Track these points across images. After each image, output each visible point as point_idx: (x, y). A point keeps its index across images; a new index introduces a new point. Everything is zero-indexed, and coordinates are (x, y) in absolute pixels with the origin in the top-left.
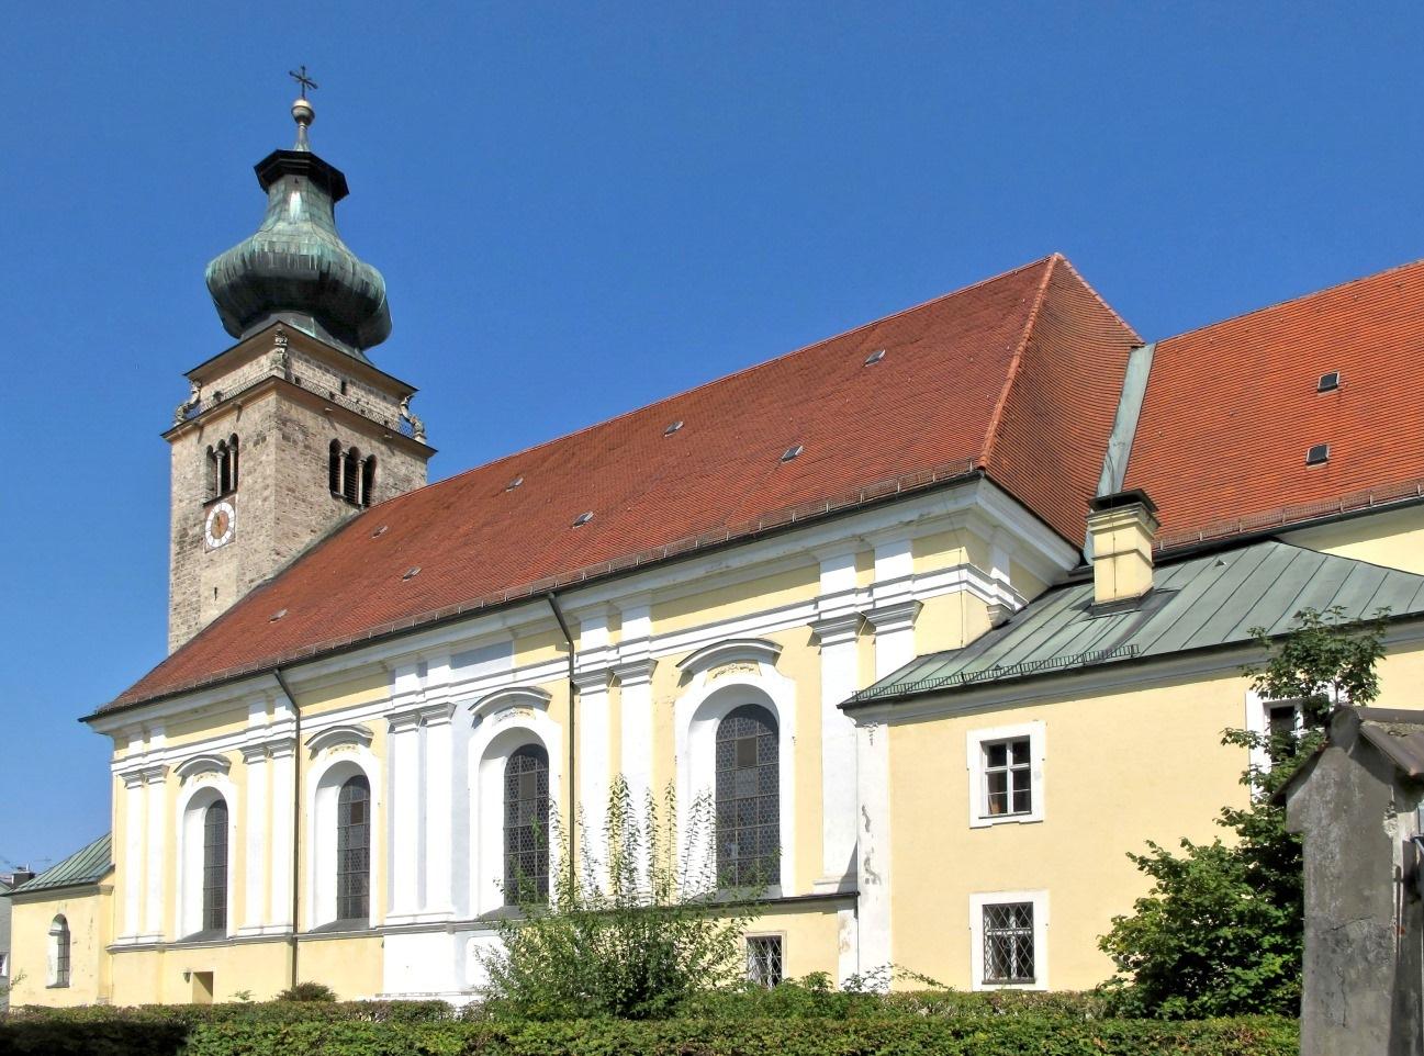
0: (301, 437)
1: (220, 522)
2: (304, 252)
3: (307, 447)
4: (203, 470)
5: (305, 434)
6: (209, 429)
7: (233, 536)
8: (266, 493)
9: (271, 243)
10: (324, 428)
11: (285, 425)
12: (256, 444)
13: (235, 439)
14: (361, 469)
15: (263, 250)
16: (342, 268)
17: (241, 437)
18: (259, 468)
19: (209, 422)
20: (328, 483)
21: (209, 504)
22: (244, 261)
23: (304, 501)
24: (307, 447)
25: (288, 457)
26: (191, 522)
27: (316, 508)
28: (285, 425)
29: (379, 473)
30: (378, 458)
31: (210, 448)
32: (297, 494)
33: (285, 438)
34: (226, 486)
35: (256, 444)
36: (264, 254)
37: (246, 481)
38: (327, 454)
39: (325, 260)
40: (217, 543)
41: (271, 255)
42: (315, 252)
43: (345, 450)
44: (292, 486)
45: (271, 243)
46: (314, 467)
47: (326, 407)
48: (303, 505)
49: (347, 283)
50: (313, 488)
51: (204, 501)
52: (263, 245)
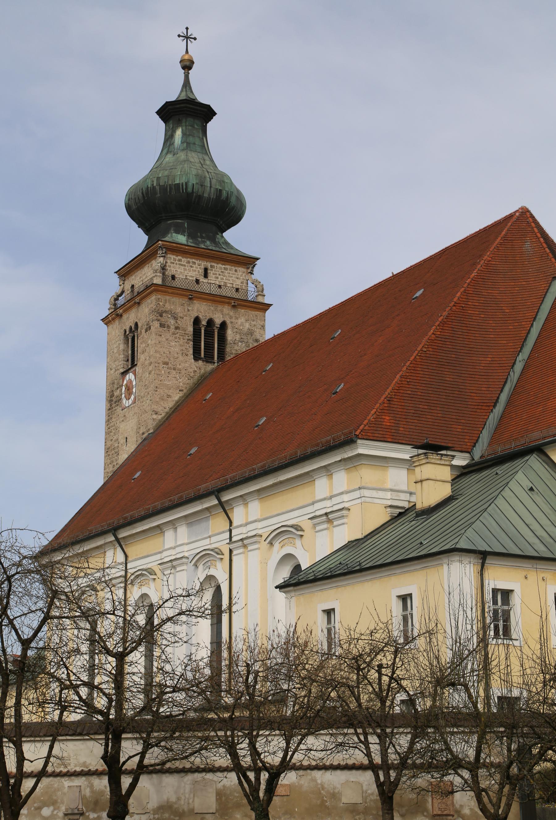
0: (172, 322)
1: (129, 389)
2: (177, 182)
3: (177, 328)
4: (122, 347)
5: (175, 318)
6: (125, 316)
7: (135, 399)
8: (150, 368)
9: (158, 178)
10: (188, 310)
11: (161, 316)
12: (146, 331)
13: (136, 324)
14: (216, 333)
15: (153, 185)
16: (202, 186)
17: (140, 325)
18: (149, 346)
19: (125, 311)
20: (191, 351)
21: (124, 373)
22: (143, 193)
23: (174, 369)
24: (177, 328)
25: (164, 339)
26: (116, 386)
27: (183, 372)
28: (161, 316)
29: (230, 334)
30: (228, 322)
31: (125, 331)
32: (170, 365)
33: (162, 325)
34: (132, 362)
35: (146, 331)
36: (154, 188)
37: (141, 358)
38: (190, 329)
39: (190, 185)
40: (130, 401)
41: (158, 188)
42: (183, 180)
43: (204, 323)
44: (167, 360)
45: (158, 178)
46: (182, 341)
47: (191, 294)
48: (174, 372)
49: (206, 195)
50: (181, 358)
51: (122, 370)
52: (153, 181)
